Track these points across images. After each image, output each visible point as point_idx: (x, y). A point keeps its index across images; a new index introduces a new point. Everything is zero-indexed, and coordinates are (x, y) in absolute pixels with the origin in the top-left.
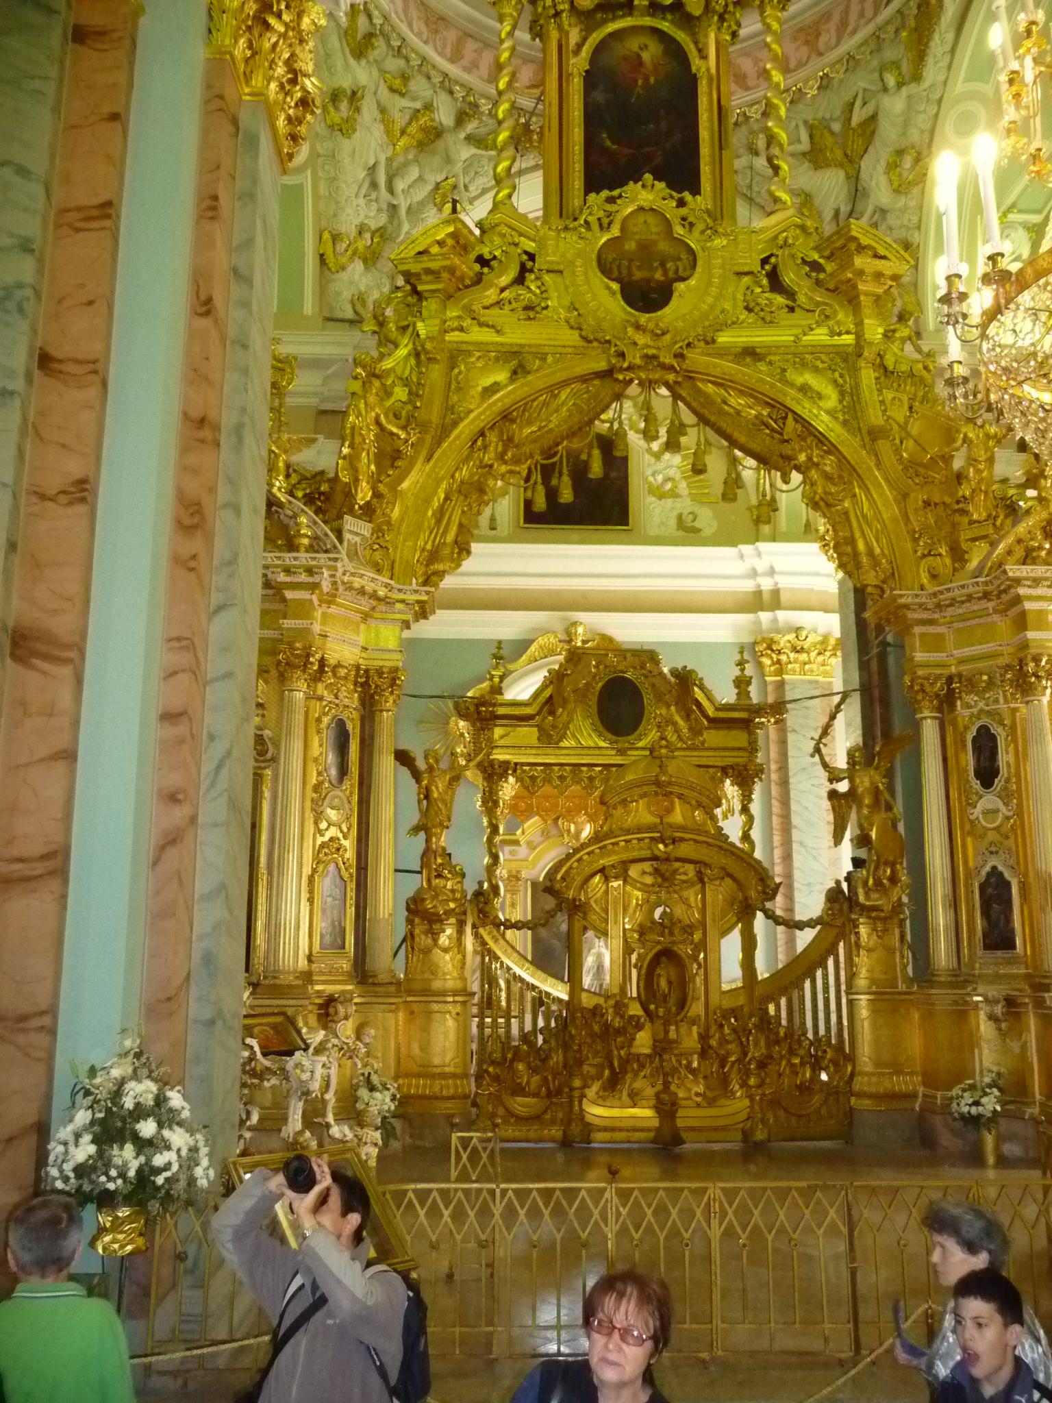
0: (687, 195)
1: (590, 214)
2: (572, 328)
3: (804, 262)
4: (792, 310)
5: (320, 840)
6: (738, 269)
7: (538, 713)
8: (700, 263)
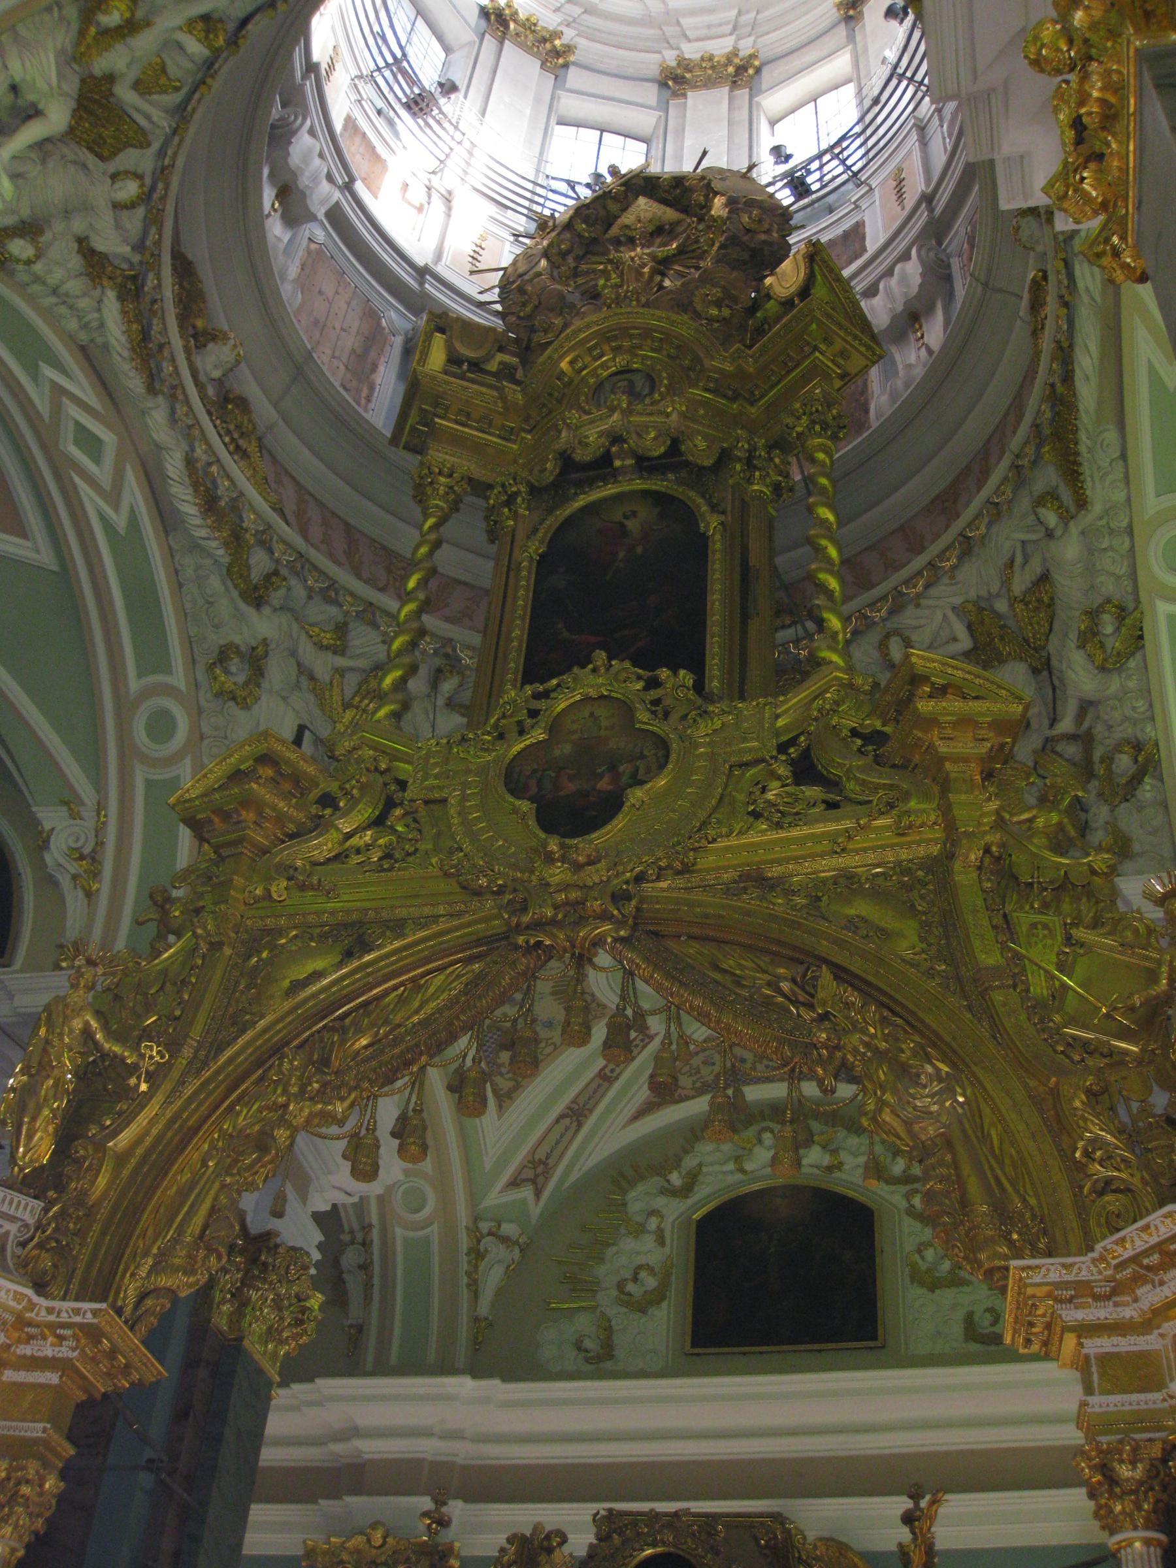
0: (664, 673)
1: (504, 716)
2: (446, 875)
3: (854, 733)
4: (831, 806)
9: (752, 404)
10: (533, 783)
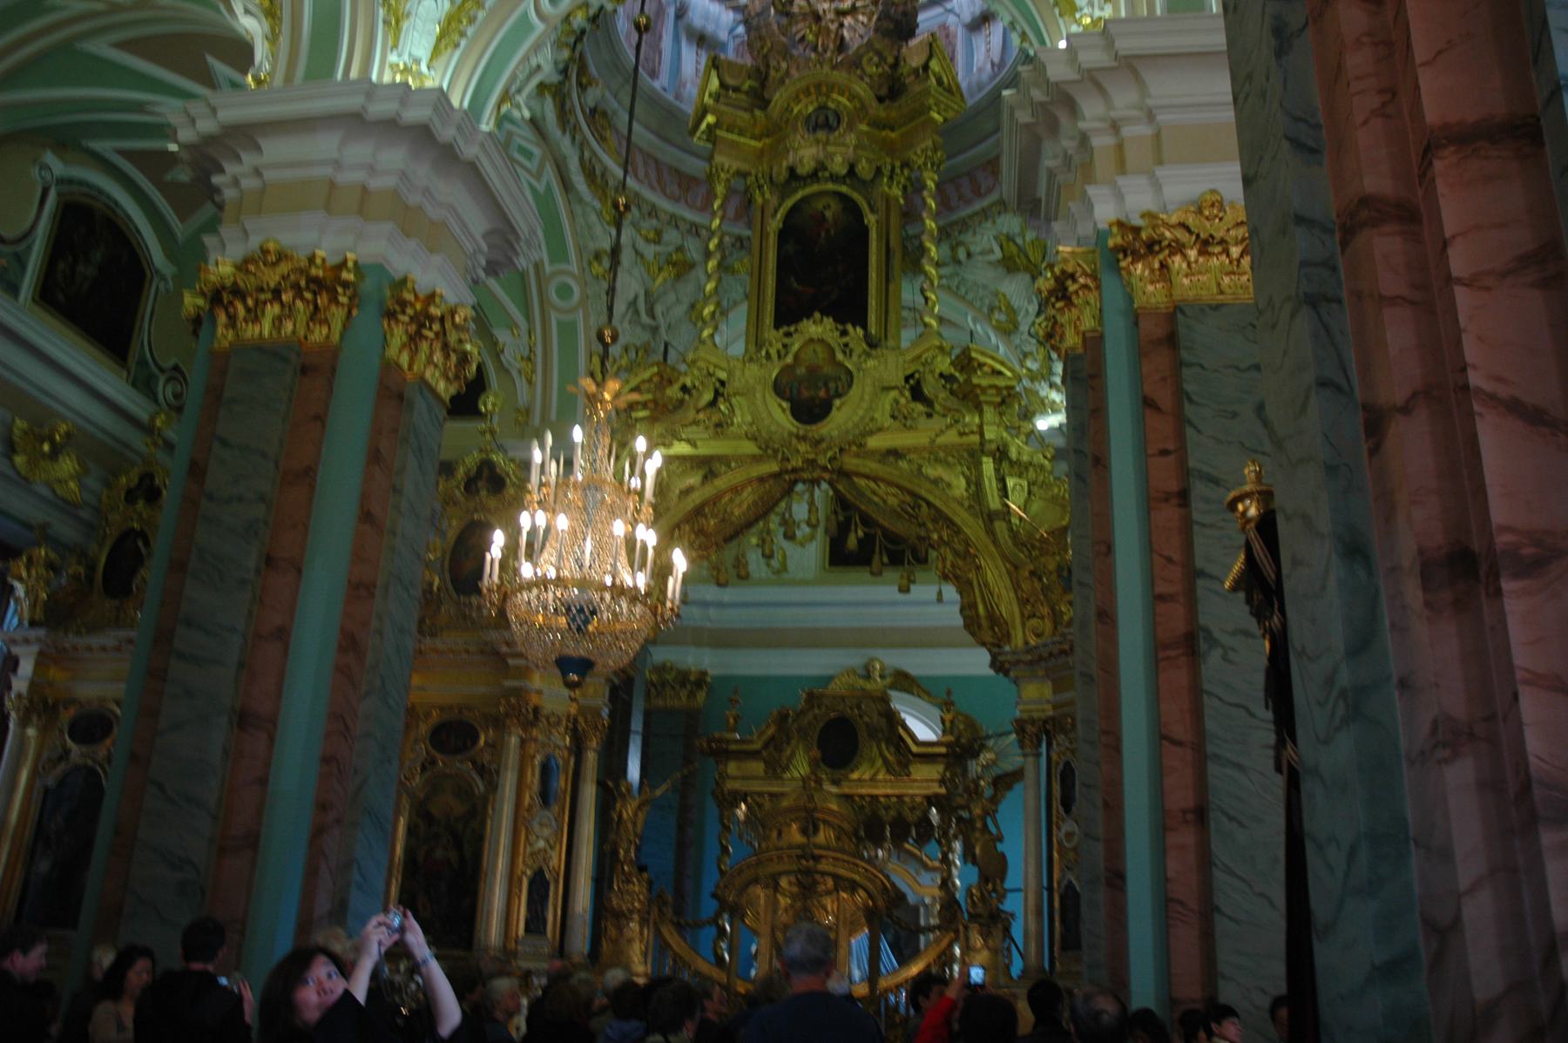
0: (849, 327)
4: (929, 415)
5: (529, 849)
6: (886, 384)
7: (766, 746)
8: (855, 381)
9: (892, 129)
10: (788, 390)
